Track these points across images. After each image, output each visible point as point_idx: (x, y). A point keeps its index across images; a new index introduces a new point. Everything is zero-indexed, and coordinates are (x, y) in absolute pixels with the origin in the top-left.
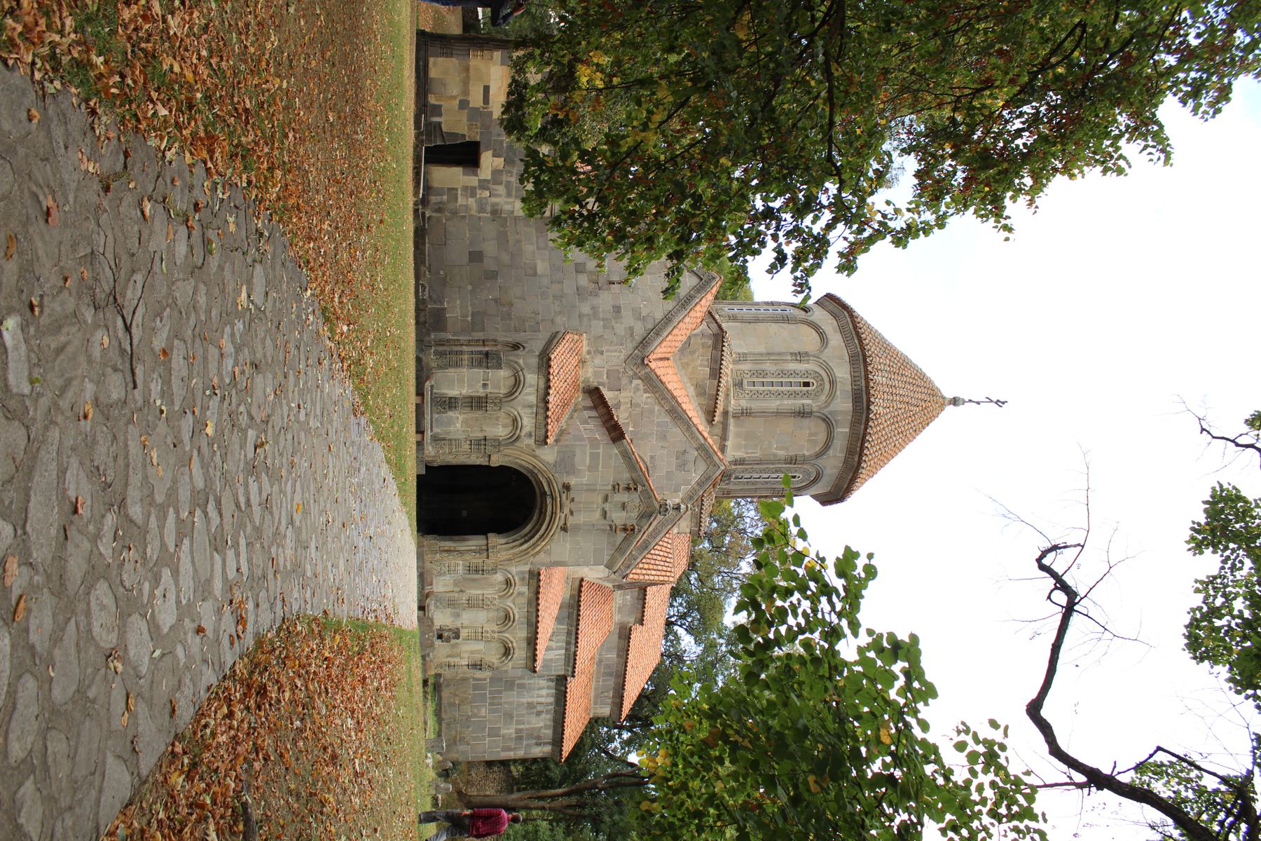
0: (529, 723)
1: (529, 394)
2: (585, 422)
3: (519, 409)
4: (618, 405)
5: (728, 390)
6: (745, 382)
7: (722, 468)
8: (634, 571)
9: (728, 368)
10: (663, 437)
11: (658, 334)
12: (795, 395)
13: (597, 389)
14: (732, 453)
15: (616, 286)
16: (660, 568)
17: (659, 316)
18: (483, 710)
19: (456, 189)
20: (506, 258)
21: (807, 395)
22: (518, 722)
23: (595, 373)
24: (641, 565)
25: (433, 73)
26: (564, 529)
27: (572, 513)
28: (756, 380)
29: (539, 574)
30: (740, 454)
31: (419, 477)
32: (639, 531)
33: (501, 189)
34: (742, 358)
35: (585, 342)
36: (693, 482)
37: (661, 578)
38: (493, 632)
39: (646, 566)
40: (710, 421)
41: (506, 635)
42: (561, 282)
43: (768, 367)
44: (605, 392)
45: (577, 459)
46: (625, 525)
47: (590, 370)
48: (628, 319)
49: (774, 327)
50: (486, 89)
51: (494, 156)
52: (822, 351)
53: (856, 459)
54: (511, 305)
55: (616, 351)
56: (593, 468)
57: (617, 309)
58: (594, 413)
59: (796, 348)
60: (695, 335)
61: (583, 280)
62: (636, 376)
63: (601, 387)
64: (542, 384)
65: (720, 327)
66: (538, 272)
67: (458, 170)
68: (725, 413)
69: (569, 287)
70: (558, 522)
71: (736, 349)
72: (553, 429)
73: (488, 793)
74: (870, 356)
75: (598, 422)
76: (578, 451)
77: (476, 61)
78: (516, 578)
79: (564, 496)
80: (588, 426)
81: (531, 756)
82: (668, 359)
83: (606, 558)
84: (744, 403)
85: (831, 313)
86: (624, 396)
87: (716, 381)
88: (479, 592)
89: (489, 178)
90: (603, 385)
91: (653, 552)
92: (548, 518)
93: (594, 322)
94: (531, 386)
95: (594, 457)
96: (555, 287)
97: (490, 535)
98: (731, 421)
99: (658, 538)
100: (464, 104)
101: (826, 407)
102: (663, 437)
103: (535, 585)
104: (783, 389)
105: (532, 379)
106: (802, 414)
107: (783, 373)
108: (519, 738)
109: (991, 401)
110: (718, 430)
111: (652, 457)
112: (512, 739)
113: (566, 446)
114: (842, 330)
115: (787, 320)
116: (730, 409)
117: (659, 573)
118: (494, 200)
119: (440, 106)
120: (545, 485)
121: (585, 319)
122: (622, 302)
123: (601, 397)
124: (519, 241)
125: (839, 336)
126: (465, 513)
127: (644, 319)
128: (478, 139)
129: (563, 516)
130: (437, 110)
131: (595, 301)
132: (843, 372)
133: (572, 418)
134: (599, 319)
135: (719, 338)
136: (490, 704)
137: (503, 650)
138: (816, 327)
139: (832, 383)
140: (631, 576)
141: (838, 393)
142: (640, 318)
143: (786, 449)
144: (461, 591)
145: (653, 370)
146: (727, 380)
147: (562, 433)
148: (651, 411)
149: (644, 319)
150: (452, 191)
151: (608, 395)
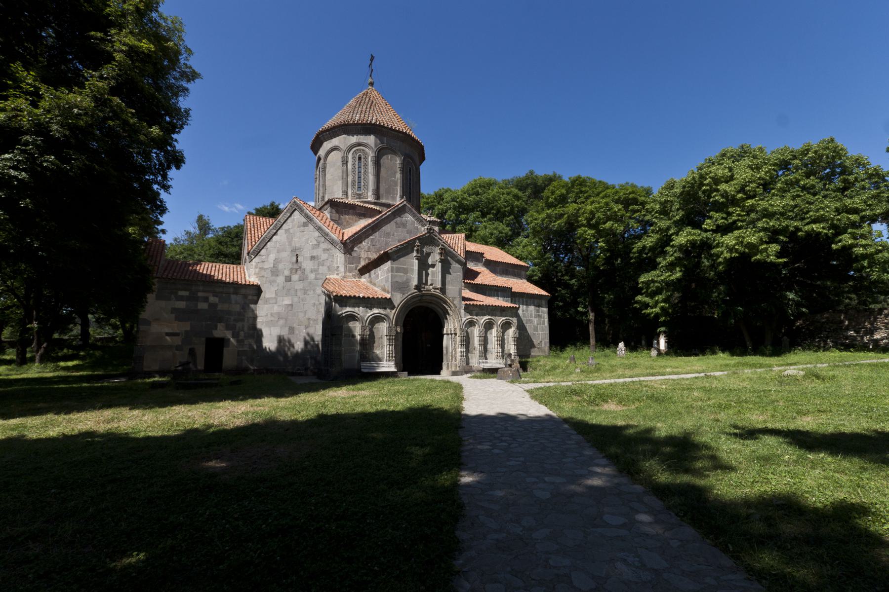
0: (532, 311)
2: (378, 276)
3: (368, 315)
4: (369, 259)
5: (362, 202)
6: (358, 192)
7: (405, 203)
9: (350, 200)
11: (327, 235)
12: (366, 165)
13: (359, 270)
15: (299, 259)
16: (457, 242)
17: (317, 234)
19: (239, 351)
21: (366, 158)
22: (531, 317)
23: (350, 272)
25: (156, 367)
27: (432, 285)
29: (466, 304)
31: (409, 374)
32: (442, 245)
33: (239, 325)
35: (332, 277)
38: (497, 331)
40: (380, 212)
41: (499, 323)
42: (296, 290)
43: (350, 179)
44: (360, 266)
45: (400, 280)
46: (439, 253)
47: (348, 274)
48: (318, 252)
49: (328, 176)
50: (168, 334)
51: (216, 329)
53: (401, 135)
54: (309, 319)
55: (337, 259)
57: (313, 258)
59: (340, 164)
60: (331, 216)
61: (295, 277)
62: (352, 249)
63: (358, 268)
66: (290, 303)
67: (226, 350)
68: (375, 204)
69: (299, 286)
70: (438, 293)
71: (340, 196)
72: (380, 294)
74: (344, 121)
76: (395, 280)
79: (422, 289)
84: (370, 193)
86: (364, 255)
89: (231, 332)
92: (434, 298)
93: (320, 271)
95: (398, 270)
96: (299, 293)
101: (372, 148)
102: (388, 235)
107: (353, 171)
109: (370, 64)
113: (392, 286)
115: (324, 169)
116: (373, 201)
118: (246, 329)
120: (415, 300)
121: (318, 276)
122: (308, 255)
124: (272, 315)
125: (334, 140)
127: (319, 243)
128: (204, 339)
129: (433, 290)
132: (354, 139)
137: (507, 325)
139: (359, 144)
141: (365, 141)
143: (396, 172)
144: (475, 349)
145: (349, 238)
146: (356, 202)
147: (384, 290)
149: (319, 243)
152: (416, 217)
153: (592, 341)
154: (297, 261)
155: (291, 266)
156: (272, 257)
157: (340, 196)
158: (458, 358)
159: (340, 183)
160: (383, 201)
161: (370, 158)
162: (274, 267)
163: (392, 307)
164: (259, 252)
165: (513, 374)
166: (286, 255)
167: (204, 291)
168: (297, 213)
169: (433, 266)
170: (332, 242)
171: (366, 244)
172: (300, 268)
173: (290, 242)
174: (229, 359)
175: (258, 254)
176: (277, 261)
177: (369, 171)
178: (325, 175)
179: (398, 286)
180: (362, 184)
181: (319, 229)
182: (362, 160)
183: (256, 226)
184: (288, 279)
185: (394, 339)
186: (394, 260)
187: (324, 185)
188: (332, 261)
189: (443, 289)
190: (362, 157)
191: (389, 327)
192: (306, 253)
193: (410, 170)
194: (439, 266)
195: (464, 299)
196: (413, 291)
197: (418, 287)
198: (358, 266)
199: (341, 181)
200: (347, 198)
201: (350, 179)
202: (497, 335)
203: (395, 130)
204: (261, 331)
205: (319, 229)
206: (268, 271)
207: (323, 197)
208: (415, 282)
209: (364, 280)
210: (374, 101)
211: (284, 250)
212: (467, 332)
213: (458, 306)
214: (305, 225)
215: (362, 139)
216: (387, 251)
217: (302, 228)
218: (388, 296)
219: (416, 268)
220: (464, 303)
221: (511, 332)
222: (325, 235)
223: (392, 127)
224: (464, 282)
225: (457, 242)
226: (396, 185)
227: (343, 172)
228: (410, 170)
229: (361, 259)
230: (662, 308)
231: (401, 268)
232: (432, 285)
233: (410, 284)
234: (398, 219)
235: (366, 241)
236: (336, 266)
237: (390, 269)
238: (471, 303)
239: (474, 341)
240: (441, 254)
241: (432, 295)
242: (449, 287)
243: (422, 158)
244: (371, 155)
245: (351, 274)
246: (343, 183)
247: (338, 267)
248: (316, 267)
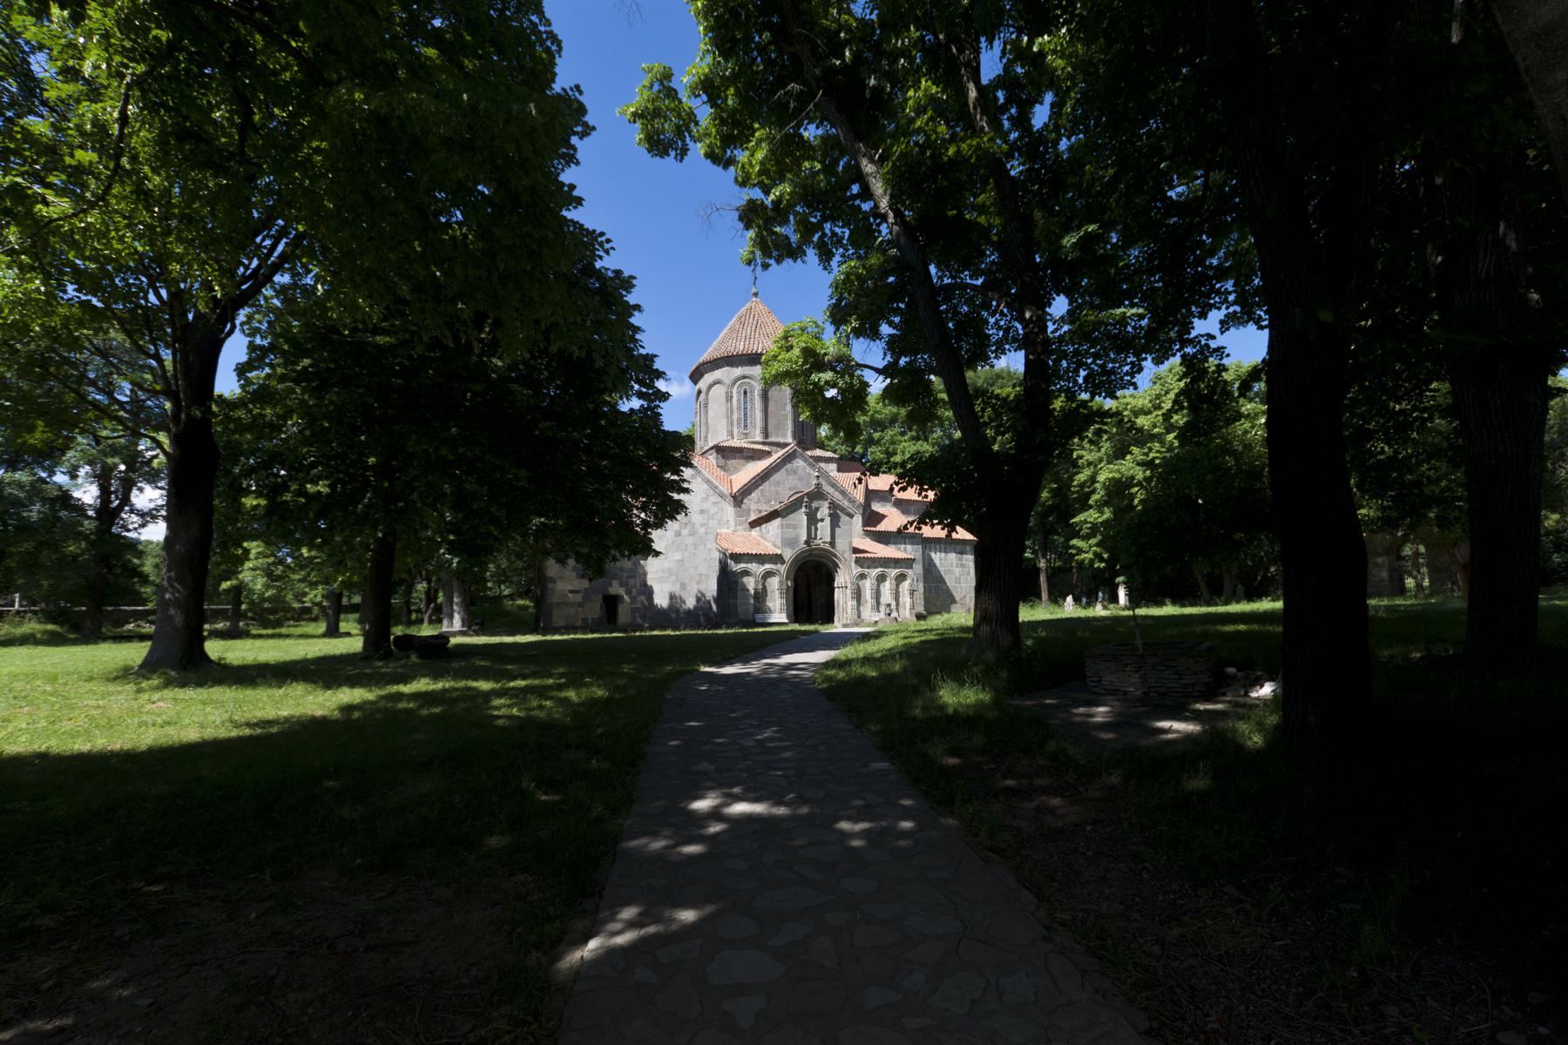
4: (760, 511)
9: (736, 443)
11: (716, 487)
14: (789, 439)
17: (705, 486)
20: (673, 578)
22: (952, 566)
23: (740, 525)
25: (562, 623)
26: (832, 543)
30: (789, 434)
33: (631, 581)
40: (769, 454)
42: (686, 545)
43: (735, 417)
45: (789, 536)
48: (707, 505)
49: (711, 413)
50: (571, 592)
57: (702, 512)
59: (723, 399)
61: (685, 532)
62: (742, 502)
65: (712, 448)
68: (764, 443)
69: (690, 540)
70: (827, 547)
77: (555, 599)
83: (847, 518)
85: (702, 376)
86: (753, 507)
95: (788, 526)
98: (769, 440)
100: (581, 605)
102: (778, 483)
104: (749, 407)
106: (765, 397)
107: (739, 408)
108: (962, 565)
110: (774, 448)
111: (790, 489)
115: (706, 405)
116: (761, 440)
118: (638, 585)
119: (583, 620)
123: (754, 521)
128: (601, 596)
130: (585, 620)
131: (697, 525)
132: (738, 371)
135: (720, 450)
138: (710, 387)
139: (744, 377)
142: (705, 499)
143: (785, 405)
147: (775, 546)
148: (762, 490)
150: (634, 610)
151: (753, 517)
153: (1045, 596)
157: (725, 438)
158: (849, 611)
159: (724, 421)
160: (771, 439)
163: (783, 562)
169: (822, 520)
170: (722, 495)
174: (623, 614)
178: (707, 412)
179: (788, 542)
181: (708, 481)
185: (785, 592)
186: (784, 517)
187: (707, 424)
194: (828, 520)
195: (856, 550)
197: (807, 543)
201: (735, 417)
204: (651, 587)
205: (708, 481)
208: (804, 538)
209: (755, 532)
215: (747, 370)
218: (779, 552)
219: (805, 523)
220: (854, 556)
222: (714, 488)
226: (786, 420)
227: (727, 410)
230: (1095, 553)
234: (789, 466)
238: (862, 555)
240: (830, 508)
241: (822, 549)
242: (838, 540)
244: (757, 388)
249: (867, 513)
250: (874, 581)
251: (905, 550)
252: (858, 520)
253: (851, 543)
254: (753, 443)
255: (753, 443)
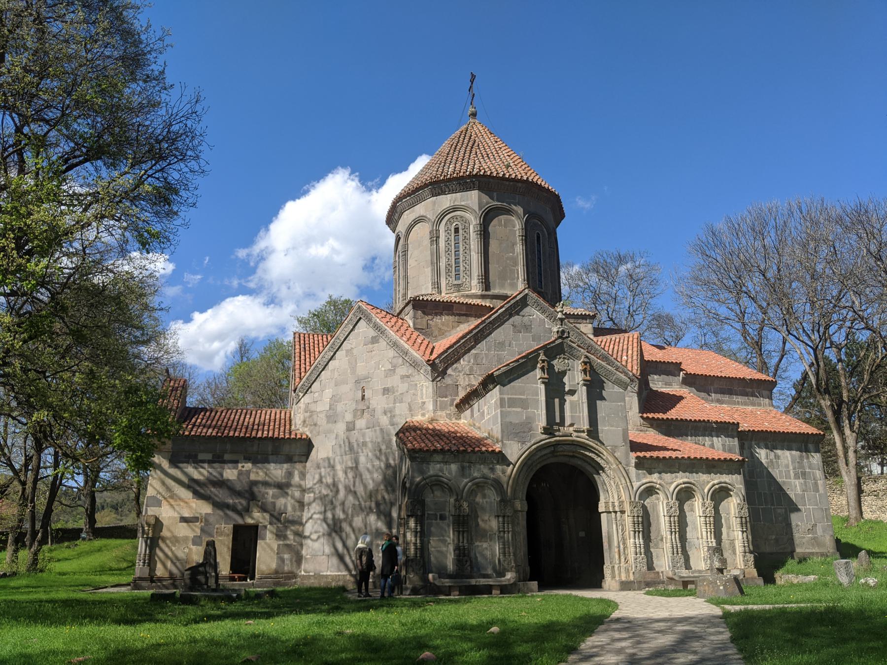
0: (787, 466)
1: (450, 473)
2: (483, 414)
5: (463, 296)
6: (456, 282)
7: (526, 291)
8: (630, 369)
9: (446, 296)
10: (501, 345)
11: (406, 353)
15: (366, 393)
16: (625, 347)
17: (391, 353)
18: (779, 511)
24: (624, 363)
27: (572, 425)
28: (454, 273)
29: (638, 458)
31: (541, 588)
34: (437, 286)
36: (542, 317)
37: (635, 345)
38: (703, 505)
39: (625, 358)
41: (706, 491)
44: (457, 400)
47: (439, 413)
48: (394, 381)
49: (411, 262)
52: (429, 219)
53: (520, 185)
55: (422, 390)
56: (524, 404)
57: (386, 391)
58: (476, 406)
59: (427, 242)
60: (414, 324)
62: (443, 373)
64: (438, 458)
68: (483, 297)
70: (584, 438)
73: (844, 502)
75: (482, 401)
76: (508, 420)
78: (644, 481)
80: (486, 411)
81: (821, 464)
82: (434, 347)
83: (617, 389)
84: (475, 282)
85: (400, 218)
87: (454, 305)
88: (662, 519)
90: (453, 400)
91: (610, 353)
93: (397, 412)
94: (441, 470)
95: (512, 403)
97: (601, 508)
99: (597, 347)
102: (501, 345)
103: (649, 462)
105: (434, 469)
107: (448, 251)
108: (804, 474)
112: (805, 483)
113: (502, 431)
114: (412, 206)
115: (405, 252)
116: (480, 293)
117: (630, 348)
120: (544, 452)
122: (380, 387)
126: (582, 534)
127: (395, 367)
129: (575, 434)
132: (446, 201)
133: (479, 428)
134: (394, 408)
136: (773, 504)
139: (455, 209)
140: (634, 371)
141: (463, 203)
143: (514, 244)
144: (662, 540)
146: (454, 297)
149: (395, 367)
151: (462, 394)
152: (547, 314)
154: (363, 397)
155: (354, 406)
156: (328, 393)
158: (631, 556)
159: (428, 271)
160: (495, 291)
161: (471, 227)
162: (330, 408)
164: (310, 387)
165: (725, 586)
166: (348, 390)
167: (232, 452)
168: (362, 323)
169: (572, 392)
170: (415, 365)
171: (466, 363)
172: (368, 408)
173: (353, 369)
175: (308, 390)
176: (335, 400)
177: (472, 247)
179: (513, 431)
180: (462, 268)
182: (461, 231)
183: (307, 348)
184: (351, 427)
186: (504, 385)
187: (406, 277)
188: (414, 395)
189: (593, 432)
190: (460, 228)
191: (501, 501)
192: (377, 384)
193: (538, 237)
194: (583, 391)
195: (635, 446)
196: (538, 436)
197: (548, 431)
198: (455, 399)
199: (429, 269)
200: (440, 292)
202: (704, 512)
203: (509, 180)
205: (395, 345)
206: (323, 416)
207: (405, 295)
208: (542, 422)
210: (477, 140)
211: (345, 382)
212: (644, 507)
213: (623, 462)
214: (374, 340)
216: (492, 373)
217: (370, 346)
219: (542, 398)
220: (633, 455)
221: (733, 506)
223: (504, 174)
224: (642, 417)
225: (625, 347)
226: (516, 264)
227: (432, 255)
228: (538, 237)
229: (460, 388)
231: (516, 399)
232: (572, 425)
233: (534, 425)
234: (516, 319)
235: (466, 357)
236: (420, 401)
237: (499, 403)
238: (648, 454)
239: (658, 523)
240: (585, 371)
242: (603, 429)
243: (559, 215)
244: (473, 222)
245: (444, 414)
246: (433, 270)
247: (424, 403)
248: (391, 405)
249: (645, 393)
250: (673, 501)
251: (712, 446)
252: (632, 402)
253: (625, 432)
254: (468, 296)
255: (468, 296)
